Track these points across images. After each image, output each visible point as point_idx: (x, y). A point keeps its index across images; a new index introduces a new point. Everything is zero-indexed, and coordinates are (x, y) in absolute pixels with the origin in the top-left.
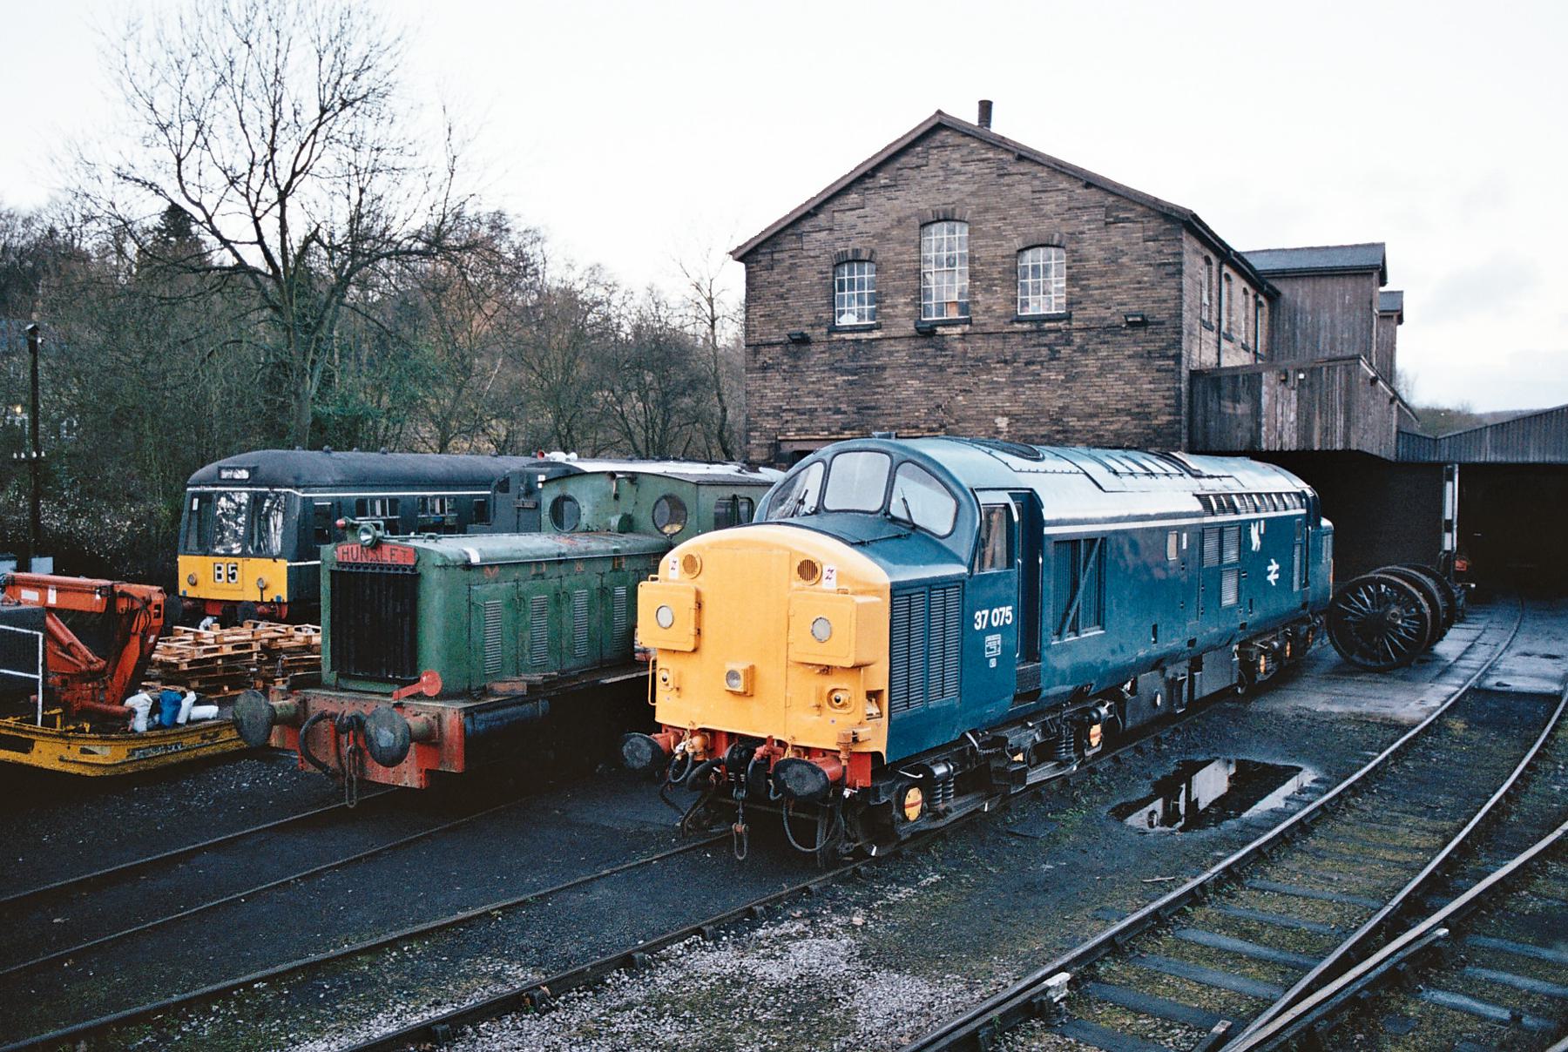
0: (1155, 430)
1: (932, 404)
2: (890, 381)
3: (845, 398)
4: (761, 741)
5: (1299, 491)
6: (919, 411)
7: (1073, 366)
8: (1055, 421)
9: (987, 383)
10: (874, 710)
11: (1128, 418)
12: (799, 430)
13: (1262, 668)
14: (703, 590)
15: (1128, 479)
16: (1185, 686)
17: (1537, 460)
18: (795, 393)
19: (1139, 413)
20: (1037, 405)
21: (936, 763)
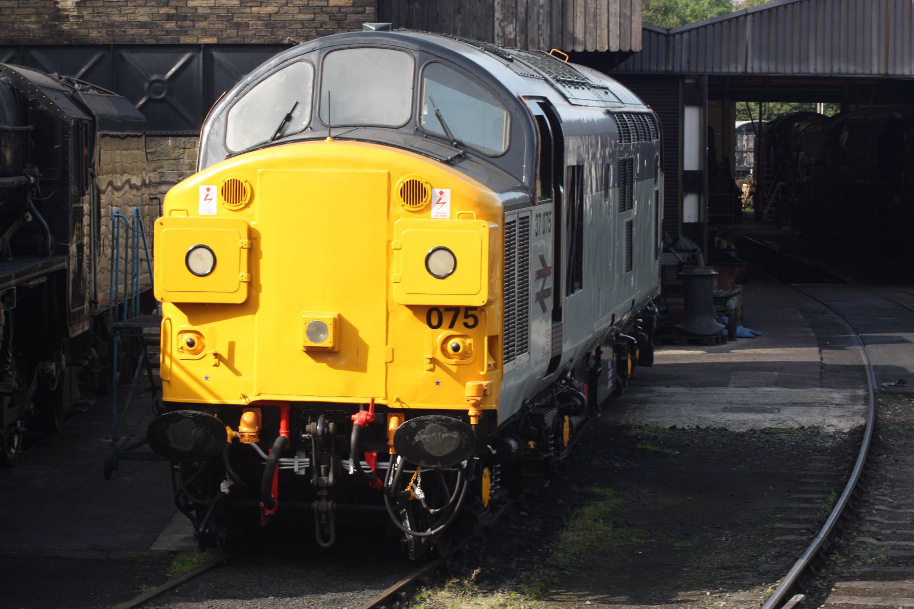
0: (332, 16)
4: (354, 408)
17: (820, 70)
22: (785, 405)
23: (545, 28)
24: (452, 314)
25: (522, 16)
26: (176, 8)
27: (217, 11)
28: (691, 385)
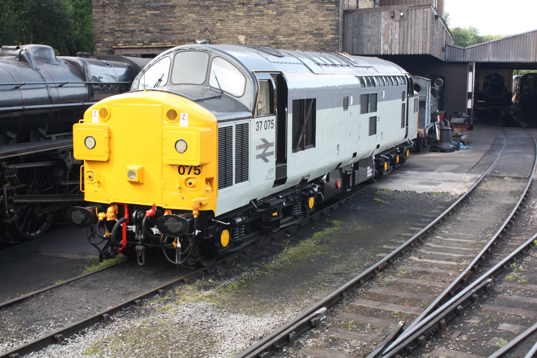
0: (325, 43)
1: (203, 28)
2: (178, 14)
3: (152, 24)
4: (149, 208)
5: (404, 75)
6: (195, 32)
7: (281, 7)
8: (272, 38)
9: (233, 16)
10: (209, 188)
11: (311, 36)
12: (125, 42)
13: (386, 168)
14: (111, 127)
15: (324, 68)
16: (351, 177)
18: (122, 20)
19: (317, 34)
20: (262, 29)
21: (237, 217)
22: (445, 181)
23: (398, 47)
24: (189, 168)
25: (390, 42)
26: (276, 41)
27: (288, 42)
28: (421, 171)
